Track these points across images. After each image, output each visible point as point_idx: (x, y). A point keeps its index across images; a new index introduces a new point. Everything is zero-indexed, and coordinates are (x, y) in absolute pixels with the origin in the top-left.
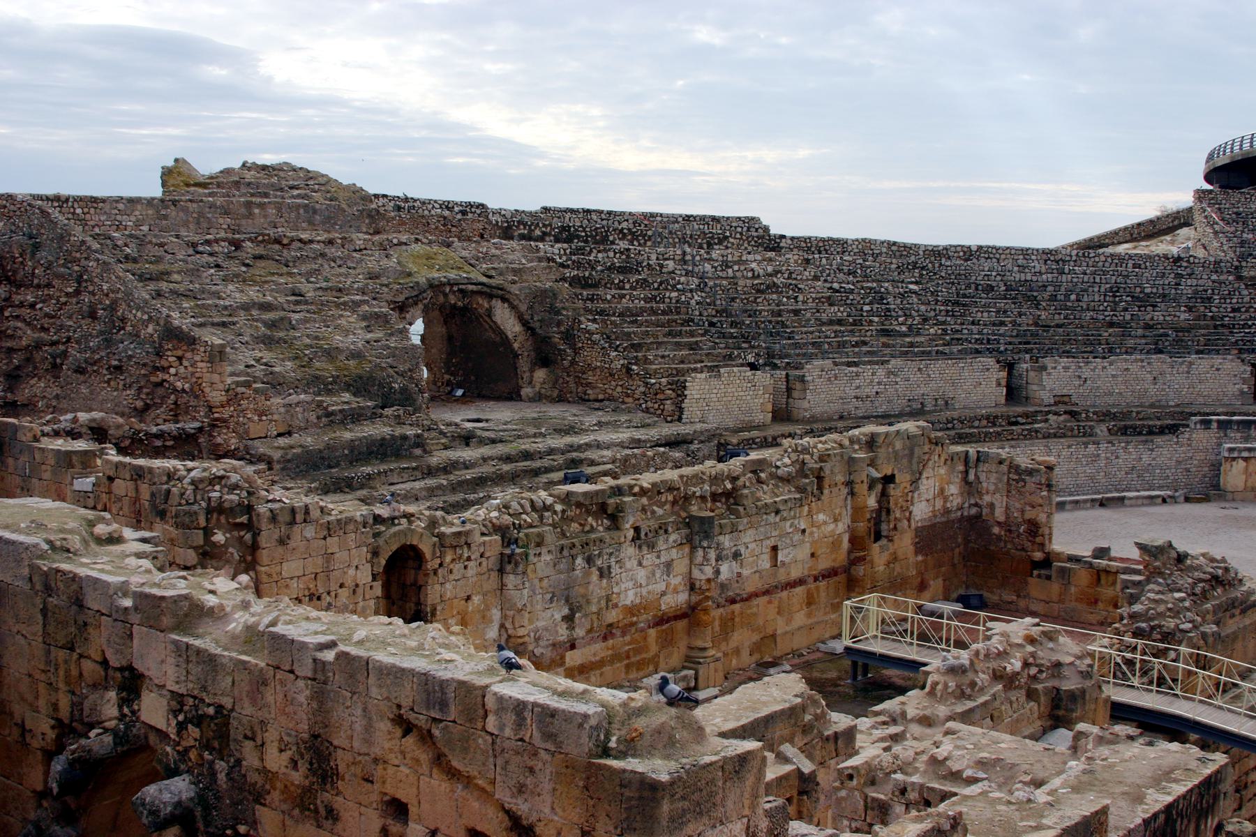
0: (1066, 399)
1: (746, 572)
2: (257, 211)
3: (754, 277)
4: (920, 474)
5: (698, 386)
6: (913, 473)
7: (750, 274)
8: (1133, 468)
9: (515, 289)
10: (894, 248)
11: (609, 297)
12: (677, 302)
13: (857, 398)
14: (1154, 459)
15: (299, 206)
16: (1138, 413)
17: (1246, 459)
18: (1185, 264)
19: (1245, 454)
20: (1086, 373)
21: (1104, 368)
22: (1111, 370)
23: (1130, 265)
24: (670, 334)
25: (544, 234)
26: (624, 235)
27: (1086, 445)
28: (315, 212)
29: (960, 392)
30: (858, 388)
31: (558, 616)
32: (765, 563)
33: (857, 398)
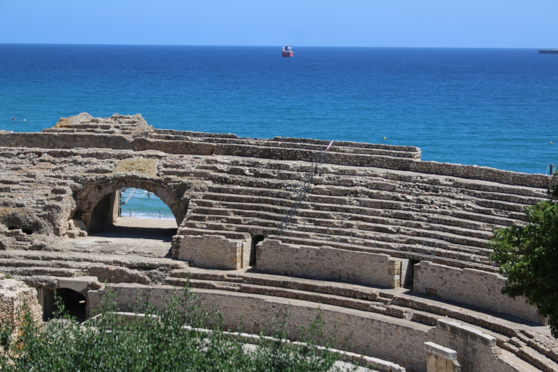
2: (79, 139)
3: (353, 186)
8: (401, 345)
10: (490, 174)
13: (296, 264)
14: (413, 342)
15: (101, 137)
17: (436, 357)
19: (434, 352)
20: (447, 277)
21: (458, 275)
24: (239, 214)
25: (252, 152)
26: (307, 155)
30: (297, 258)
33: (296, 264)
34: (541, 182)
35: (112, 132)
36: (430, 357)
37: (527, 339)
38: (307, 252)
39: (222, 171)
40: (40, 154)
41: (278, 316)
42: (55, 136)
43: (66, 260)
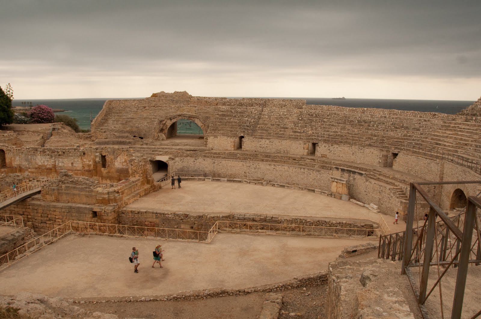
0: (325, 156)
1: (65, 165)
4: (117, 157)
5: (211, 140)
6: (114, 156)
7: (278, 115)
9: (200, 116)
11: (227, 119)
12: (247, 121)
14: (321, 177)
16: (334, 163)
17: (337, 182)
18: (437, 117)
22: (339, 149)
23: (419, 116)
27: (301, 168)
28: (174, 101)
29: (292, 149)
31: (26, 164)
32: (70, 165)
34: (361, 111)
35: (174, 98)
36: (333, 183)
37: (379, 173)
38: (265, 142)
39: (223, 111)
40: (145, 107)
41: (255, 168)
42: (152, 100)
43: (158, 148)
